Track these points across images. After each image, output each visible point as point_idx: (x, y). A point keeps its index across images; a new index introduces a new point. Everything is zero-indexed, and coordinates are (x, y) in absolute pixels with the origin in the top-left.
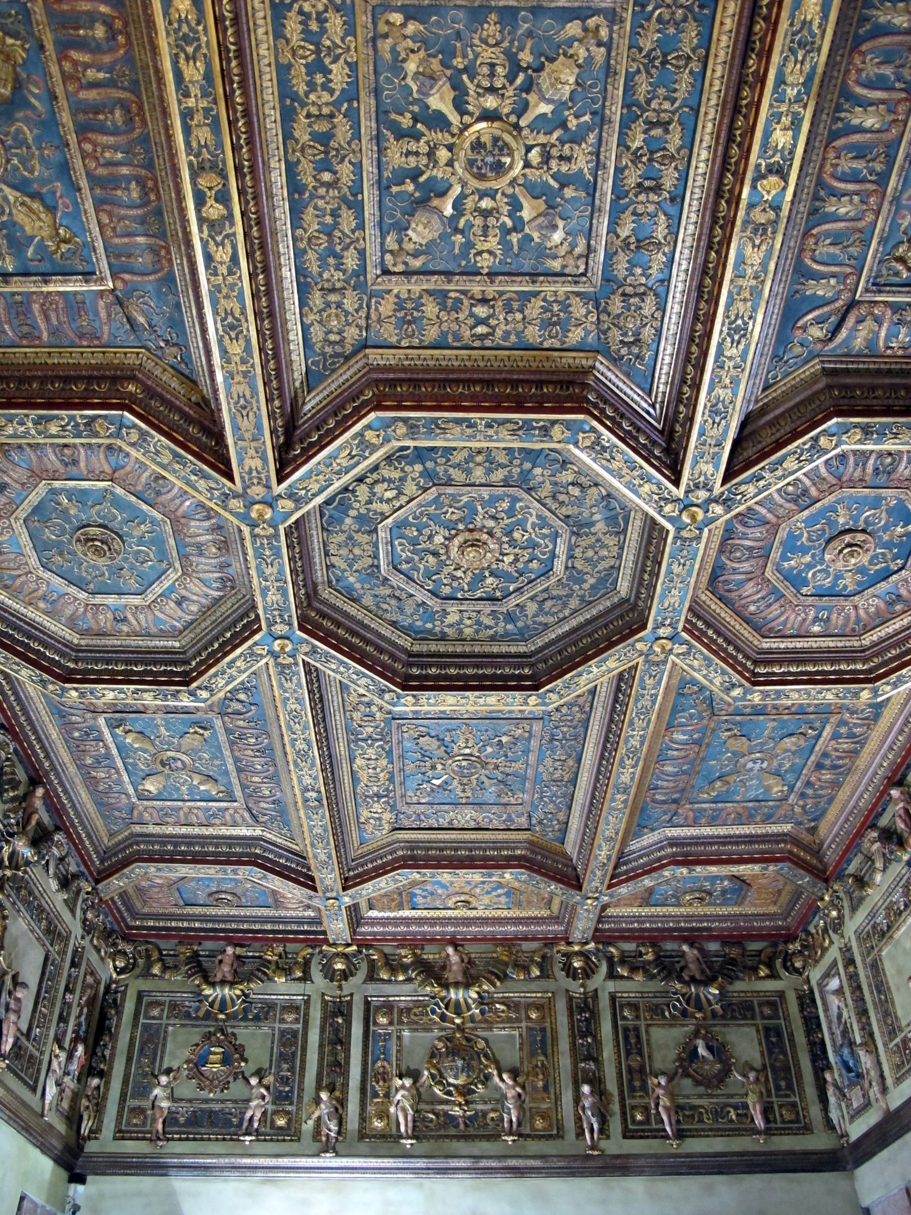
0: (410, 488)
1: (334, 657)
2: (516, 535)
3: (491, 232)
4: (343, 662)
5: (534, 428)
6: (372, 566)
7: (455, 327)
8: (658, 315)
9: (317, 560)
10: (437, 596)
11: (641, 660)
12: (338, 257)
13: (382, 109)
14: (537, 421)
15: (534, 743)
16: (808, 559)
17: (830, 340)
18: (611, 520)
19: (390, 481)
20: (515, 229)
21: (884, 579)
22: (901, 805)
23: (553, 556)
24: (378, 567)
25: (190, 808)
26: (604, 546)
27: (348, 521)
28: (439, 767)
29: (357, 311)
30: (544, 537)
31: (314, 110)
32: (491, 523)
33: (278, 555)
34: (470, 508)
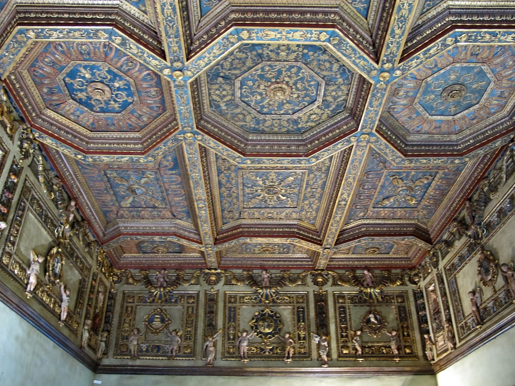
9: (354, 90)
24: (326, 84)
30: (247, 97)
34: (280, 72)
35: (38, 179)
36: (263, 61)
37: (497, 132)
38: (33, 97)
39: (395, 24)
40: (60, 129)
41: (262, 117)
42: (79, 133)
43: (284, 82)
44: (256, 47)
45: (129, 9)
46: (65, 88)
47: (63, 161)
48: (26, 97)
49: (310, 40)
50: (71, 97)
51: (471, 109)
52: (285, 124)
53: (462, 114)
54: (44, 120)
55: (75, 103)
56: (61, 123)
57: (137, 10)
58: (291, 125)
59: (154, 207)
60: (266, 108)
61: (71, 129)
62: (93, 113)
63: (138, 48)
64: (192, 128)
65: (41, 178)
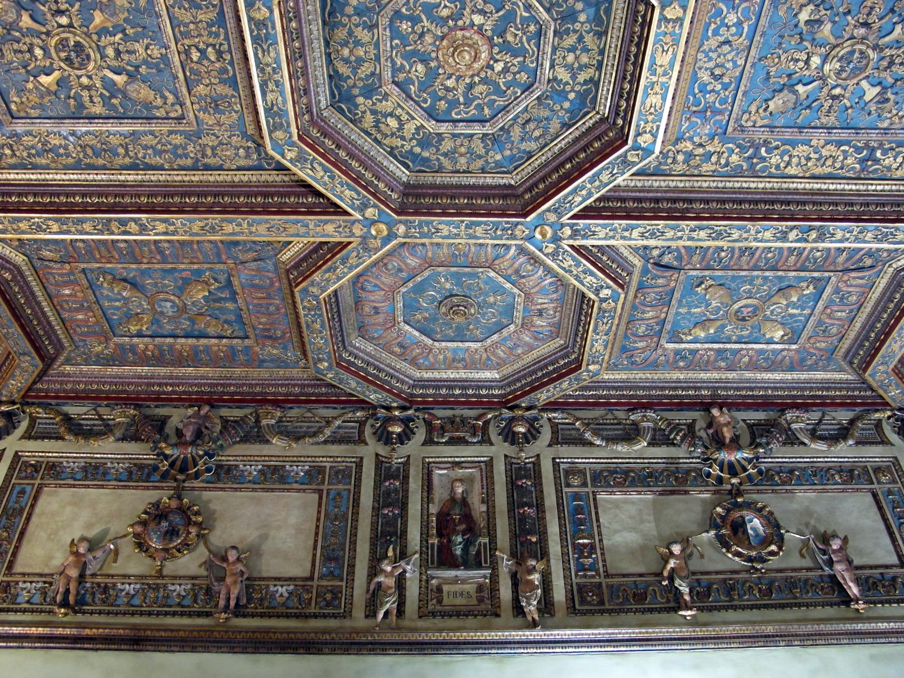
0: (387, 106)
1: (567, 196)
3: (130, 48)
4: (575, 191)
6: (483, 141)
7: (214, 73)
10: (532, 85)
12: (176, 147)
13: (72, 115)
14: (251, 31)
19: (377, 122)
20: (123, 31)
24: (485, 135)
25: (823, 312)
27: (426, 154)
28: (837, 91)
29: (218, 137)
31: (81, 155)
32: (428, 39)
33: (428, 223)
37: (389, 383)
39: (648, 228)
41: (384, 21)
43: (492, 62)
44: (593, 9)
49: (639, 120)
51: (424, 337)
52: (366, 69)
53: (411, 330)
58: (360, 84)
60: (413, 27)
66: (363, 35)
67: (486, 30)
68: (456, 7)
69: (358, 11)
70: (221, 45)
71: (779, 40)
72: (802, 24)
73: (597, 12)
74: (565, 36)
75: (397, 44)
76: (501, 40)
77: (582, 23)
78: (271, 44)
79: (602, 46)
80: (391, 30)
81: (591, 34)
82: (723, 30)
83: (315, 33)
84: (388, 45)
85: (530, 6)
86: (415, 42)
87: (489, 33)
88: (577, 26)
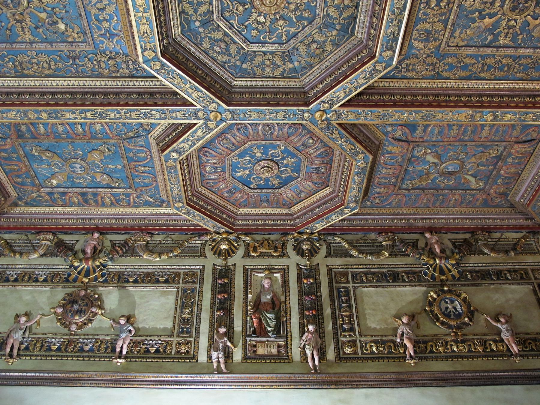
2: (281, 22)
5: (392, 43)
8: (421, 77)
11: (199, 107)
15: (62, 46)
16: (259, 155)
17: (393, 138)
18: (294, 70)
21: (243, 184)
22: (95, 243)
23: (263, 43)
26: (273, 70)
30: (280, 36)
35: (351, 256)
36: (213, 20)
38: (271, 215)
40: (311, 211)
41: (318, 20)
42: (324, 197)
44: (192, 28)
45: (158, 132)
46: (263, 190)
47: (366, 219)
48: (265, 220)
50: (276, 189)
54: (298, 217)
55: (284, 188)
56: (308, 206)
57: (159, 126)
59: (499, 158)
61: (318, 201)
62: (299, 179)
63: (183, 142)
64: (308, 111)
65: (355, 253)
66: (333, 12)
67: (256, 13)
68: (274, 26)
69: (333, 26)
70: (424, 8)
71: (67, 9)
72: (60, 21)
73: (189, 27)
74: (206, 11)
75: (313, 3)
76: (246, 7)
77: (197, 20)
78: (388, 37)
79: (181, 5)
80: (316, 12)
81: (190, 13)
82: (107, 17)
83: (362, 15)
84: (318, 4)
85: (230, 28)
86: (301, 5)
87: (254, 11)
88: (200, 18)
